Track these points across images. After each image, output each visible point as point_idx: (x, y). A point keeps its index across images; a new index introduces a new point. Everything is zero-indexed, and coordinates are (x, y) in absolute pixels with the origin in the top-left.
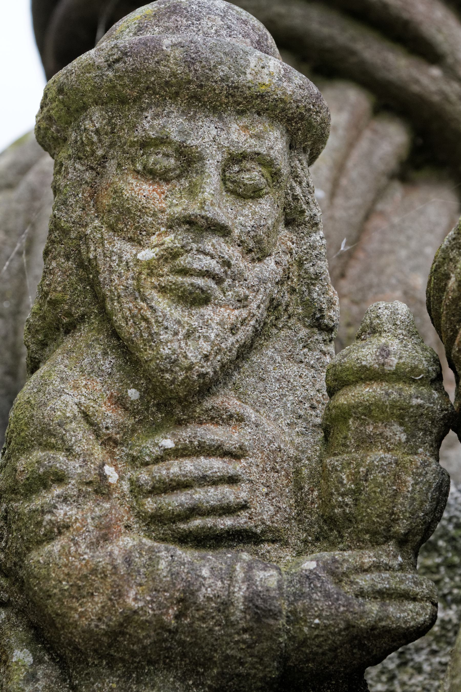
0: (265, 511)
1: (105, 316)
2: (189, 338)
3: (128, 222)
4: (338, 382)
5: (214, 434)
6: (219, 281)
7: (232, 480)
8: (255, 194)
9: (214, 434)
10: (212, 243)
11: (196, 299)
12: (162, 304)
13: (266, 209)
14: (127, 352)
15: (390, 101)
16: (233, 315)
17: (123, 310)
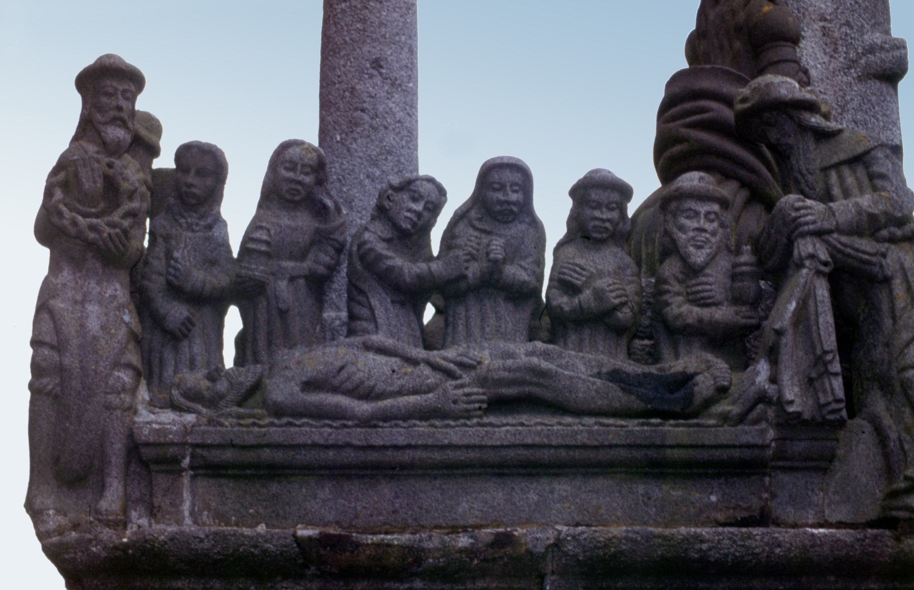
0: (719, 297)
1: (679, 252)
2: (699, 257)
3: (682, 228)
4: (735, 266)
5: (704, 279)
6: (705, 243)
7: (711, 291)
8: (712, 221)
9: (704, 279)
10: (703, 235)
11: (700, 247)
12: (691, 249)
13: (715, 224)
14: (684, 259)
15: (744, 184)
16: (708, 251)
17: (682, 251)
